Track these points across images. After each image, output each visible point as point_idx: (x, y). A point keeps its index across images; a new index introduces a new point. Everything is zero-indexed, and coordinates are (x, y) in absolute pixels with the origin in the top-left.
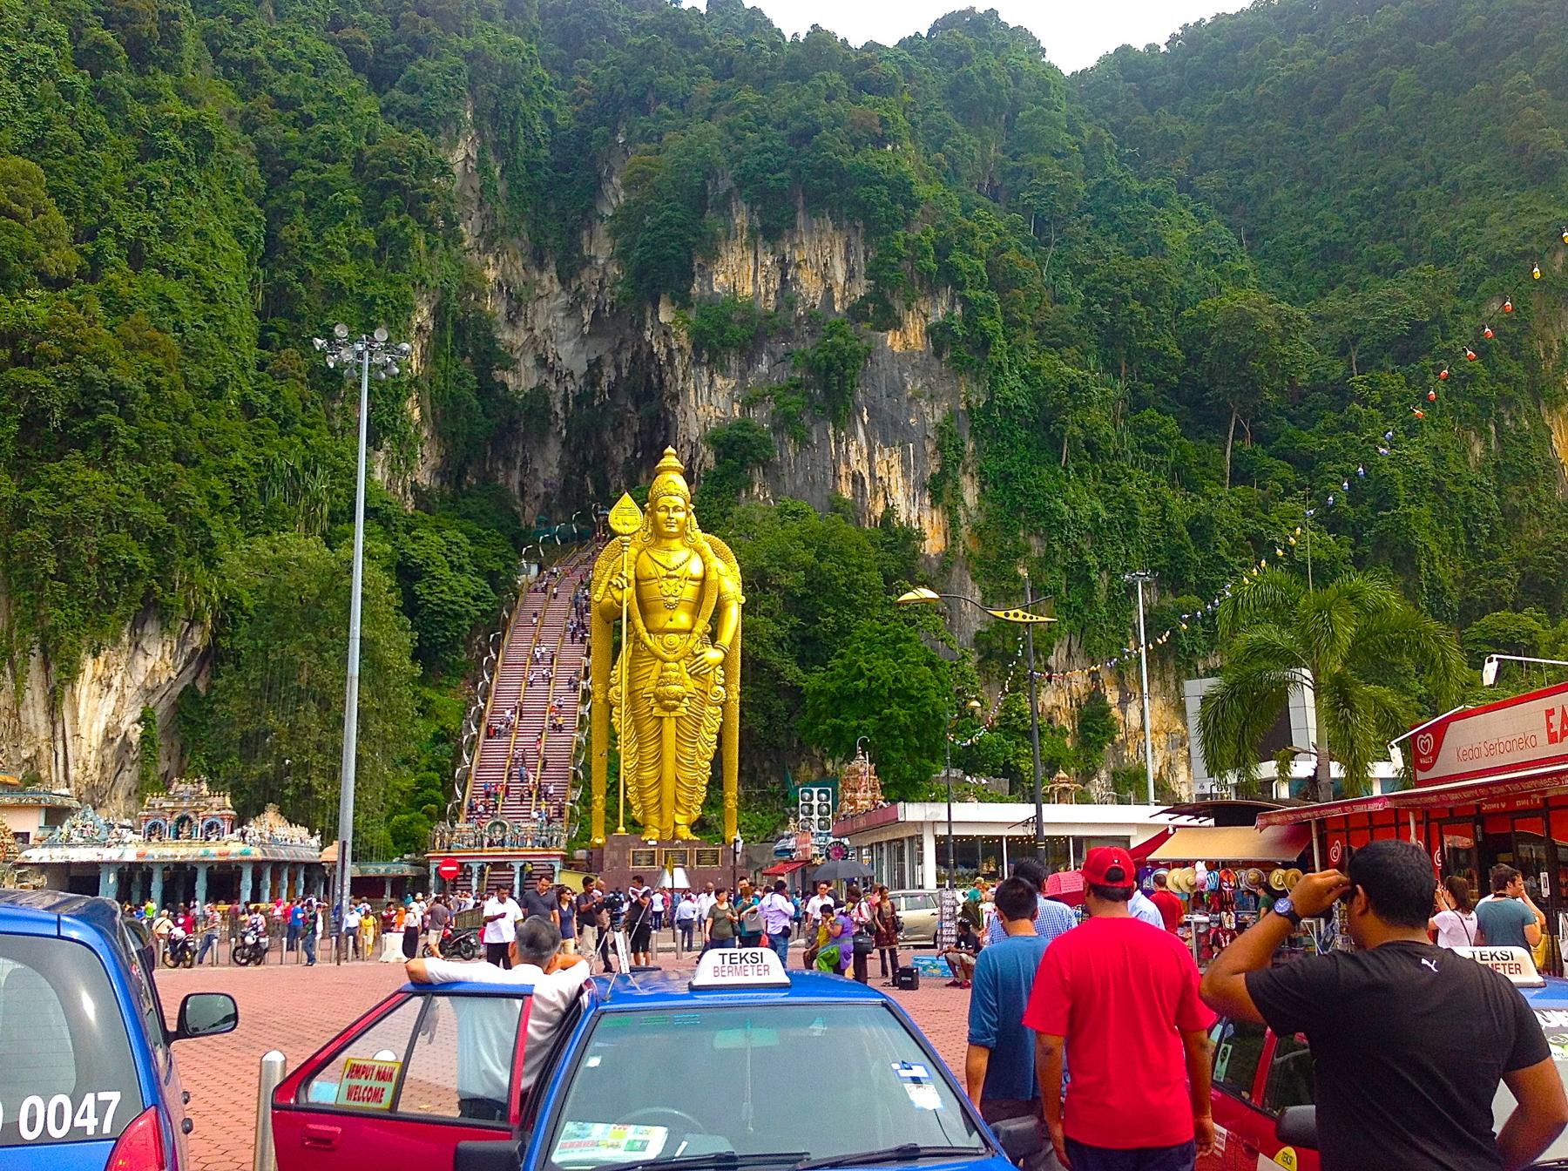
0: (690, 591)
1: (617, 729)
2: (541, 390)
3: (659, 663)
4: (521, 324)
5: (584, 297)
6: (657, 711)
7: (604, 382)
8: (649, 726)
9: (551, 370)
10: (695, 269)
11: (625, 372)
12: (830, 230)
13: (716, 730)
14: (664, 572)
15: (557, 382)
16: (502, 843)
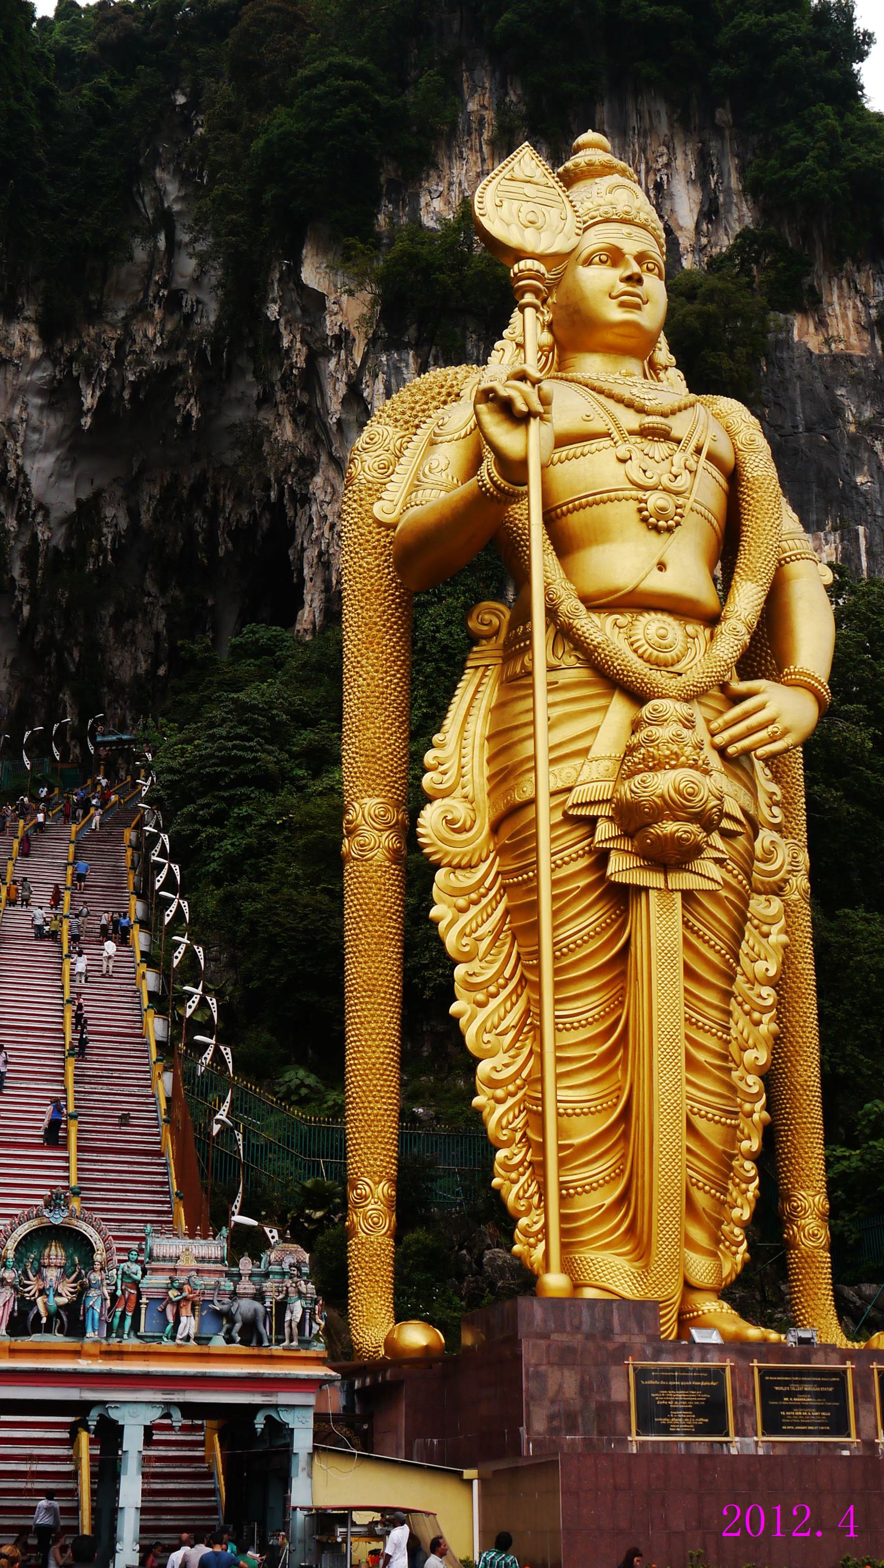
0: (707, 491)
1: (451, 942)
5: (90, 369)
6: (621, 868)
9: (11, 497)
11: (145, 519)
15: (21, 519)
16: (71, 1320)
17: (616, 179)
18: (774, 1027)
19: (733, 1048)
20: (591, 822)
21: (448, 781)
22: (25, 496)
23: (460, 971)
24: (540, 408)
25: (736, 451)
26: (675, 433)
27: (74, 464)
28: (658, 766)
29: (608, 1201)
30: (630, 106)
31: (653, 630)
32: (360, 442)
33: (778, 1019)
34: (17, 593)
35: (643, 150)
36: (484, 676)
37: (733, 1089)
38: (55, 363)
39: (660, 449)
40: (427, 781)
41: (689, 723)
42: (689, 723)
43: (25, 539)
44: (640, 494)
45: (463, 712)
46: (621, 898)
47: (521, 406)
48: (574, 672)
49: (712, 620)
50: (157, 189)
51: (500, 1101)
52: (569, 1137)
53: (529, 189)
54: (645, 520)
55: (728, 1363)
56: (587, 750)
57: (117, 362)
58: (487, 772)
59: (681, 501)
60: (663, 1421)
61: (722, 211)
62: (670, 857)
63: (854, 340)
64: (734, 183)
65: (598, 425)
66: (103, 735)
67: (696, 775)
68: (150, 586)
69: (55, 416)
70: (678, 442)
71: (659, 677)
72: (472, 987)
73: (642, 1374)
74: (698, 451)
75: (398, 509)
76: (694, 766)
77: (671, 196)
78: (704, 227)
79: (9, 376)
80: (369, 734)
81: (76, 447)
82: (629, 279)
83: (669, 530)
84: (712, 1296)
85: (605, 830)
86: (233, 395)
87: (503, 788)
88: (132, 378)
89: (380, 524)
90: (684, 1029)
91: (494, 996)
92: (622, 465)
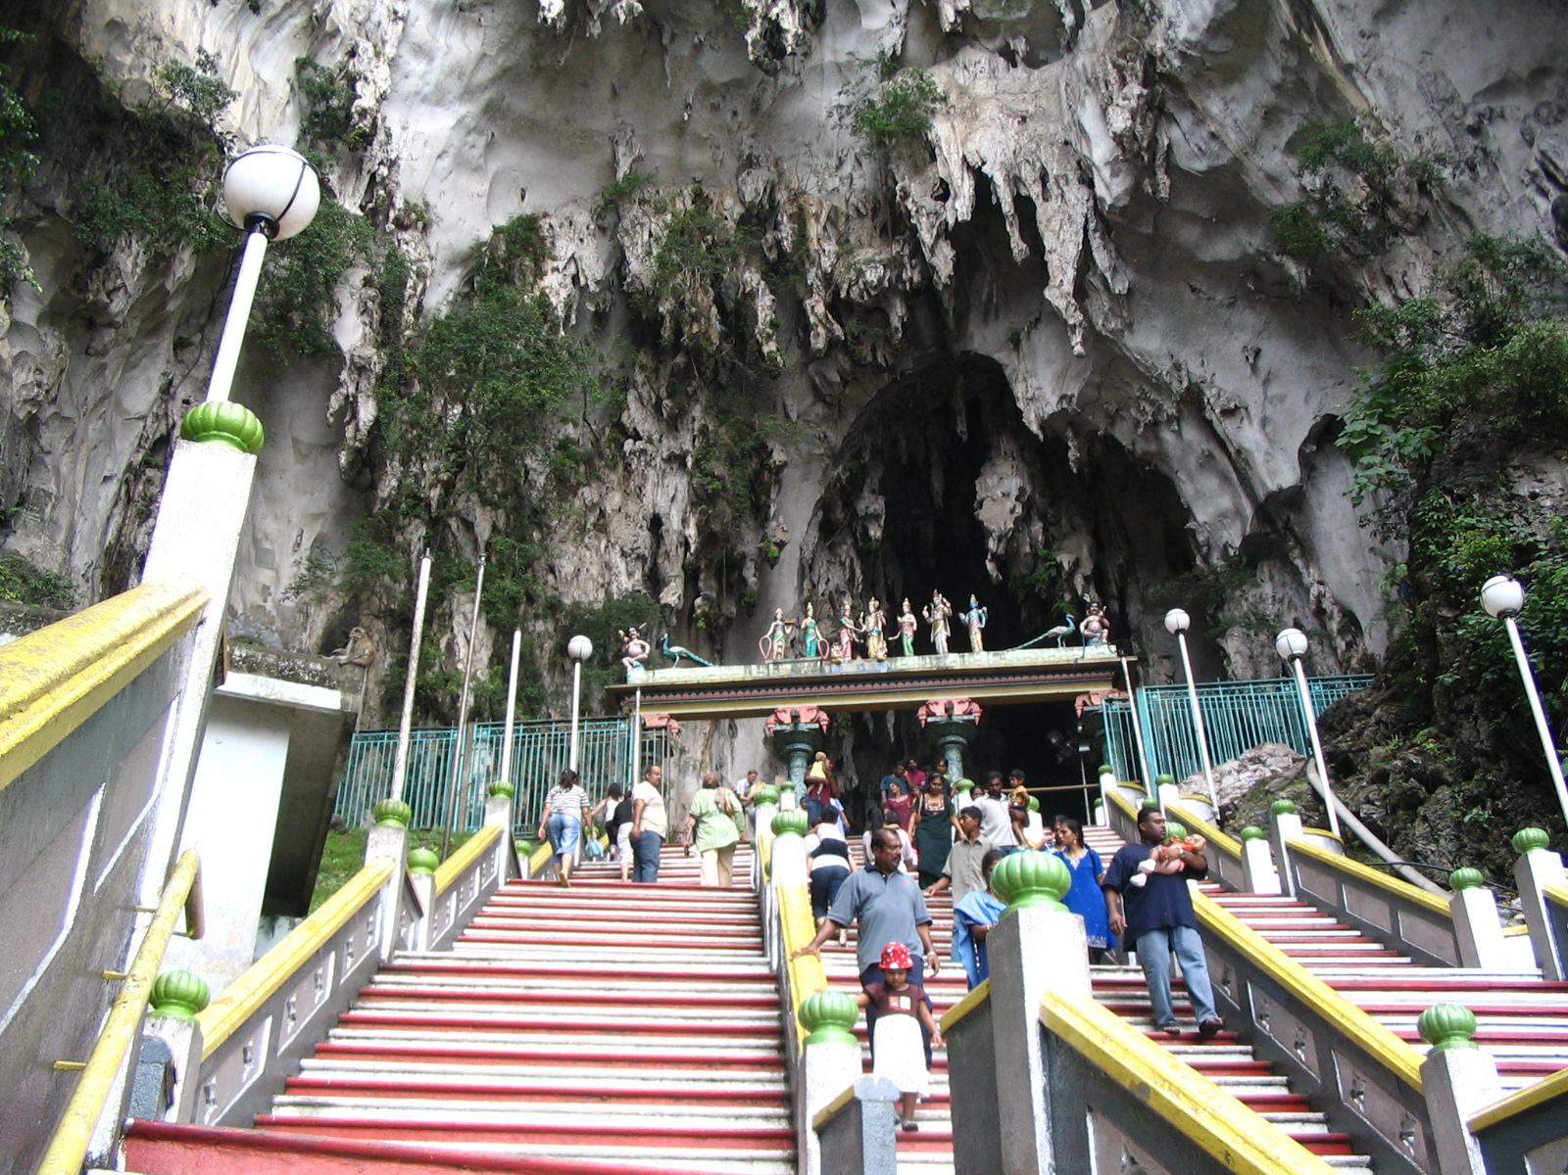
22: (384, 171)
34: (344, 376)
66: (648, 664)
68: (636, 415)
69: (465, 35)
86: (828, 57)
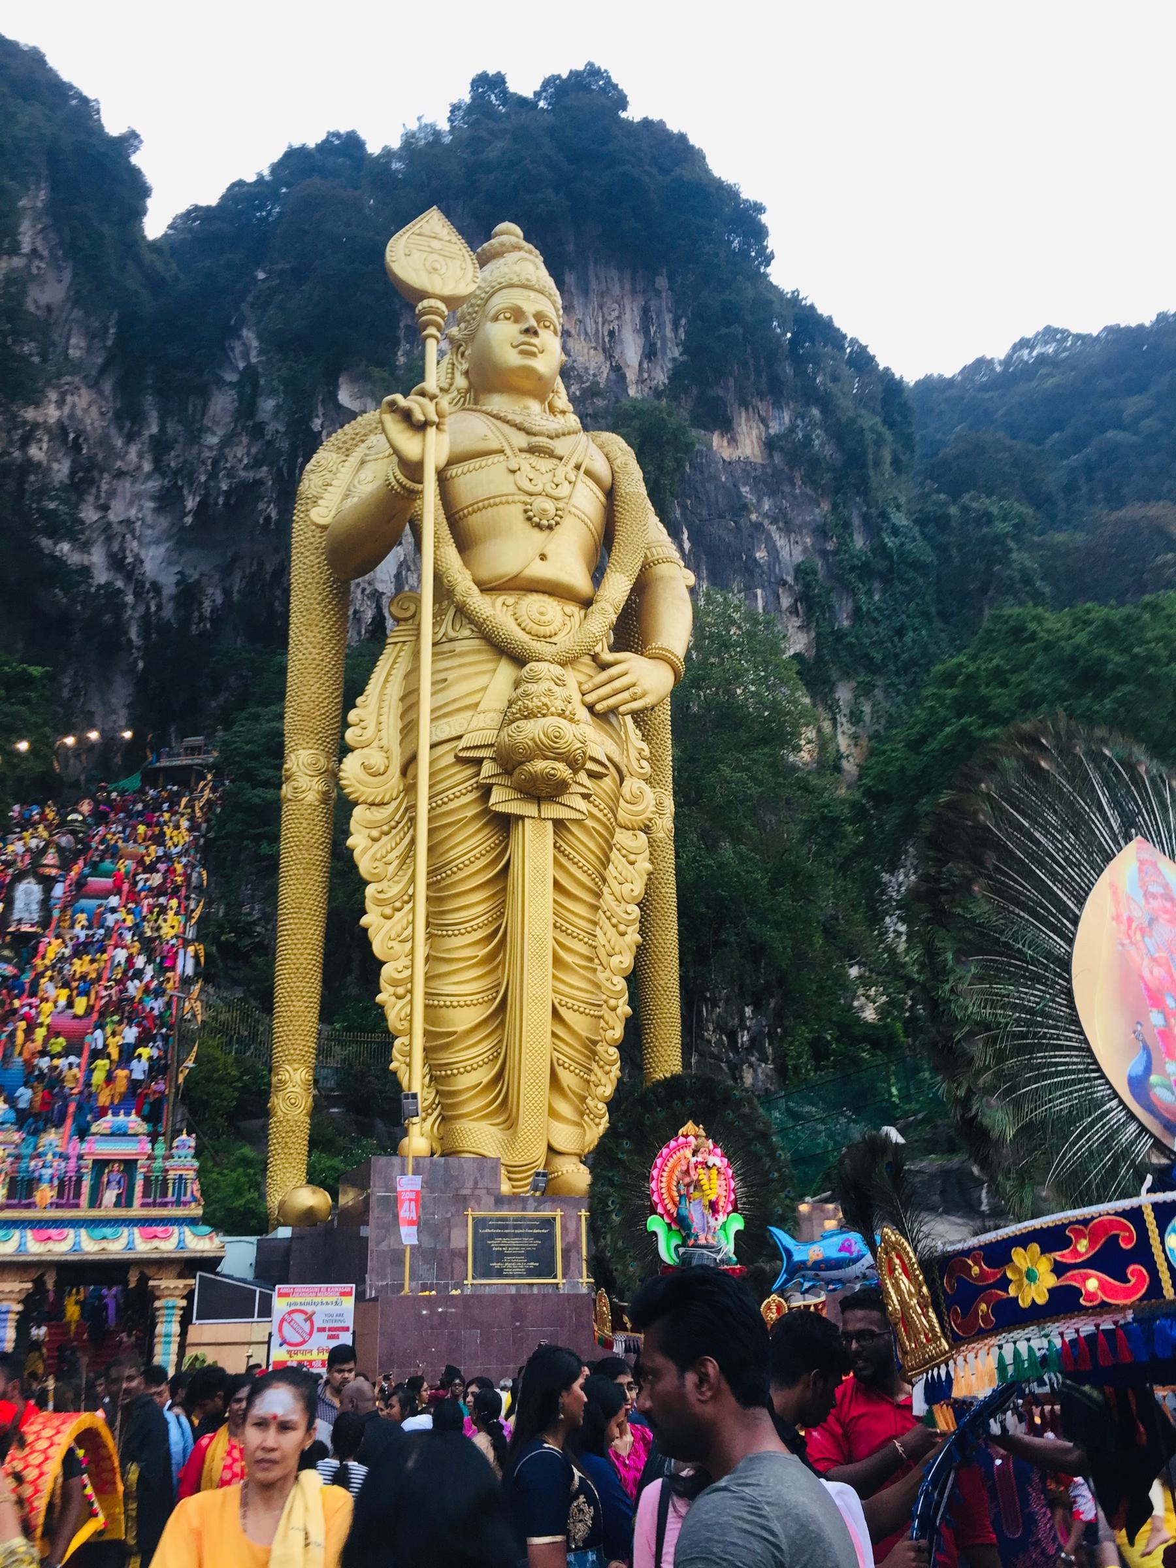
0: (586, 501)
1: (365, 866)
2: (111, 594)
3: (505, 672)
4: (91, 499)
6: (502, 800)
7: (207, 607)
8: (471, 847)
10: (402, 333)
12: (616, 290)
13: (638, 889)
14: (521, 440)
15: (136, 594)
17: (522, 254)
18: (638, 938)
19: (602, 952)
20: (478, 762)
21: (369, 733)
23: (370, 891)
24: (436, 419)
25: (613, 473)
26: (558, 452)
27: (180, 554)
28: (529, 715)
29: (485, 1080)
30: (591, 274)
31: (535, 608)
32: (308, 467)
33: (642, 932)
35: (601, 307)
36: (401, 650)
37: (598, 986)
38: (163, 475)
39: (545, 464)
40: (350, 735)
41: (560, 682)
42: (560, 682)
43: (141, 609)
44: (528, 499)
45: (382, 679)
46: (504, 825)
47: (419, 416)
48: (467, 642)
49: (586, 603)
50: (244, 344)
51: (399, 997)
52: (454, 1025)
53: (436, 244)
54: (529, 519)
55: (559, 1213)
56: (477, 704)
57: (213, 476)
58: (400, 725)
59: (561, 505)
60: (496, 1265)
61: (659, 355)
62: (543, 791)
63: (757, 451)
64: (669, 333)
65: (494, 445)
67: (564, 723)
70: (561, 459)
71: (539, 647)
72: (380, 903)
73: (479, 1223)
74: (578, 467)
75: (332, 514)
76: (562, 714)
77: (621, 342)
78: (645, 366)
79: (128, 485)
80: (306, 698)
81: (183, 541)
82: (527, 331)
83: (550, 528)
84: (575, 1159)
85: (488, 768)
87: (410, 738)
88: (225, 488)
89: (318, 526)
90: (550, 933)
91: (399, 910)
92: (511, 476)
